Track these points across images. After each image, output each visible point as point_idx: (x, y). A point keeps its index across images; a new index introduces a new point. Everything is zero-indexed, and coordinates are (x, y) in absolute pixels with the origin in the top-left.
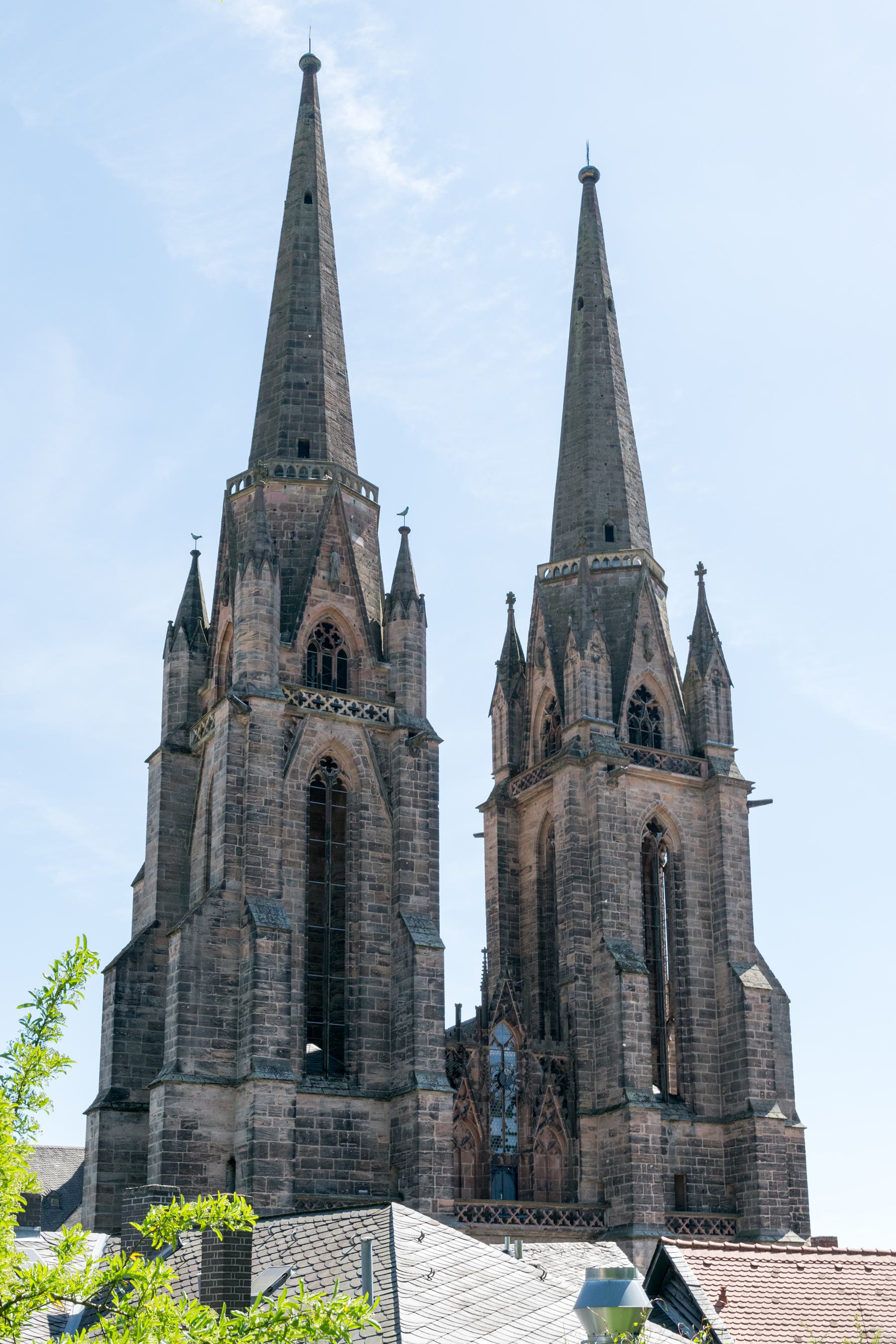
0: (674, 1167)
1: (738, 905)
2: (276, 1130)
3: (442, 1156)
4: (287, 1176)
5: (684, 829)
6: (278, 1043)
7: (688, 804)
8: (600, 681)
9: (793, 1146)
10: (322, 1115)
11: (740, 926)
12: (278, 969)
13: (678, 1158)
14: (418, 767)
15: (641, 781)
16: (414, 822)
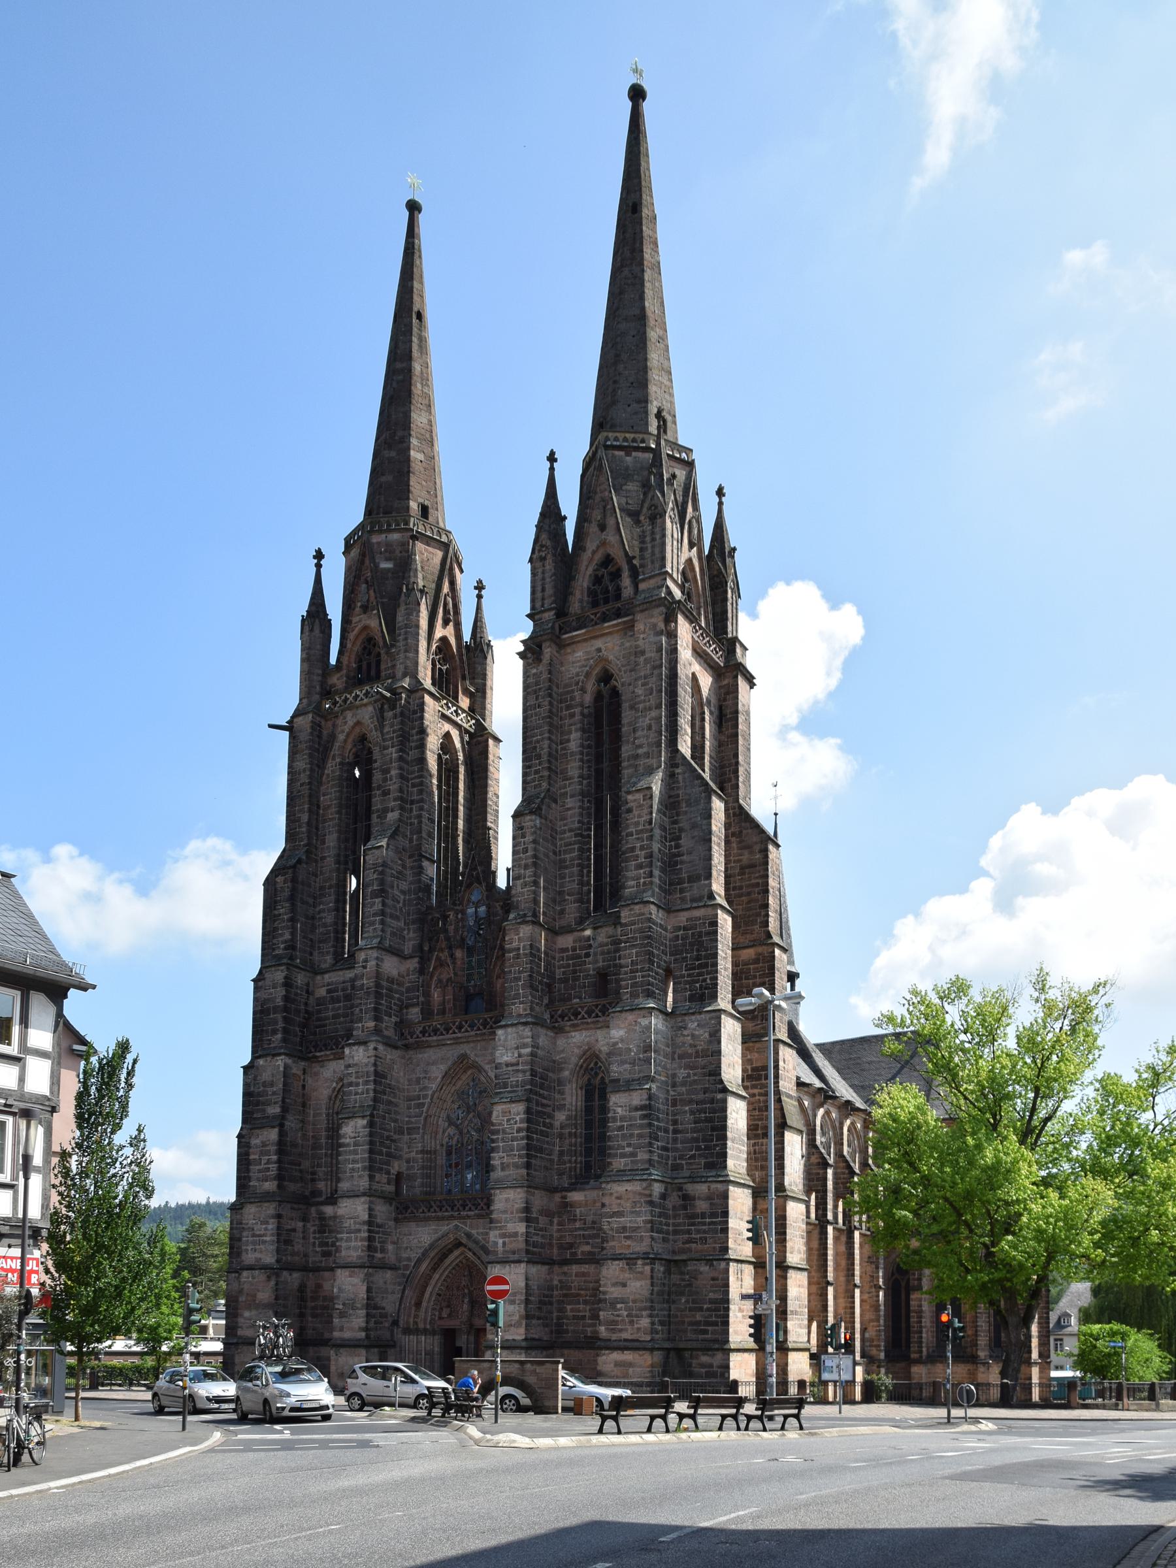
0: (596, 966)
3: (368, 993)
4: (281, 1025)
5: (623, 669)
6: (286, 942)
7: (628, 644)
9: (705, 923)
10: (344, 982)
11: (648, 737)
12: (287, 893)
14: (395, 716)
15: (585, 644)
16: (391, 758)
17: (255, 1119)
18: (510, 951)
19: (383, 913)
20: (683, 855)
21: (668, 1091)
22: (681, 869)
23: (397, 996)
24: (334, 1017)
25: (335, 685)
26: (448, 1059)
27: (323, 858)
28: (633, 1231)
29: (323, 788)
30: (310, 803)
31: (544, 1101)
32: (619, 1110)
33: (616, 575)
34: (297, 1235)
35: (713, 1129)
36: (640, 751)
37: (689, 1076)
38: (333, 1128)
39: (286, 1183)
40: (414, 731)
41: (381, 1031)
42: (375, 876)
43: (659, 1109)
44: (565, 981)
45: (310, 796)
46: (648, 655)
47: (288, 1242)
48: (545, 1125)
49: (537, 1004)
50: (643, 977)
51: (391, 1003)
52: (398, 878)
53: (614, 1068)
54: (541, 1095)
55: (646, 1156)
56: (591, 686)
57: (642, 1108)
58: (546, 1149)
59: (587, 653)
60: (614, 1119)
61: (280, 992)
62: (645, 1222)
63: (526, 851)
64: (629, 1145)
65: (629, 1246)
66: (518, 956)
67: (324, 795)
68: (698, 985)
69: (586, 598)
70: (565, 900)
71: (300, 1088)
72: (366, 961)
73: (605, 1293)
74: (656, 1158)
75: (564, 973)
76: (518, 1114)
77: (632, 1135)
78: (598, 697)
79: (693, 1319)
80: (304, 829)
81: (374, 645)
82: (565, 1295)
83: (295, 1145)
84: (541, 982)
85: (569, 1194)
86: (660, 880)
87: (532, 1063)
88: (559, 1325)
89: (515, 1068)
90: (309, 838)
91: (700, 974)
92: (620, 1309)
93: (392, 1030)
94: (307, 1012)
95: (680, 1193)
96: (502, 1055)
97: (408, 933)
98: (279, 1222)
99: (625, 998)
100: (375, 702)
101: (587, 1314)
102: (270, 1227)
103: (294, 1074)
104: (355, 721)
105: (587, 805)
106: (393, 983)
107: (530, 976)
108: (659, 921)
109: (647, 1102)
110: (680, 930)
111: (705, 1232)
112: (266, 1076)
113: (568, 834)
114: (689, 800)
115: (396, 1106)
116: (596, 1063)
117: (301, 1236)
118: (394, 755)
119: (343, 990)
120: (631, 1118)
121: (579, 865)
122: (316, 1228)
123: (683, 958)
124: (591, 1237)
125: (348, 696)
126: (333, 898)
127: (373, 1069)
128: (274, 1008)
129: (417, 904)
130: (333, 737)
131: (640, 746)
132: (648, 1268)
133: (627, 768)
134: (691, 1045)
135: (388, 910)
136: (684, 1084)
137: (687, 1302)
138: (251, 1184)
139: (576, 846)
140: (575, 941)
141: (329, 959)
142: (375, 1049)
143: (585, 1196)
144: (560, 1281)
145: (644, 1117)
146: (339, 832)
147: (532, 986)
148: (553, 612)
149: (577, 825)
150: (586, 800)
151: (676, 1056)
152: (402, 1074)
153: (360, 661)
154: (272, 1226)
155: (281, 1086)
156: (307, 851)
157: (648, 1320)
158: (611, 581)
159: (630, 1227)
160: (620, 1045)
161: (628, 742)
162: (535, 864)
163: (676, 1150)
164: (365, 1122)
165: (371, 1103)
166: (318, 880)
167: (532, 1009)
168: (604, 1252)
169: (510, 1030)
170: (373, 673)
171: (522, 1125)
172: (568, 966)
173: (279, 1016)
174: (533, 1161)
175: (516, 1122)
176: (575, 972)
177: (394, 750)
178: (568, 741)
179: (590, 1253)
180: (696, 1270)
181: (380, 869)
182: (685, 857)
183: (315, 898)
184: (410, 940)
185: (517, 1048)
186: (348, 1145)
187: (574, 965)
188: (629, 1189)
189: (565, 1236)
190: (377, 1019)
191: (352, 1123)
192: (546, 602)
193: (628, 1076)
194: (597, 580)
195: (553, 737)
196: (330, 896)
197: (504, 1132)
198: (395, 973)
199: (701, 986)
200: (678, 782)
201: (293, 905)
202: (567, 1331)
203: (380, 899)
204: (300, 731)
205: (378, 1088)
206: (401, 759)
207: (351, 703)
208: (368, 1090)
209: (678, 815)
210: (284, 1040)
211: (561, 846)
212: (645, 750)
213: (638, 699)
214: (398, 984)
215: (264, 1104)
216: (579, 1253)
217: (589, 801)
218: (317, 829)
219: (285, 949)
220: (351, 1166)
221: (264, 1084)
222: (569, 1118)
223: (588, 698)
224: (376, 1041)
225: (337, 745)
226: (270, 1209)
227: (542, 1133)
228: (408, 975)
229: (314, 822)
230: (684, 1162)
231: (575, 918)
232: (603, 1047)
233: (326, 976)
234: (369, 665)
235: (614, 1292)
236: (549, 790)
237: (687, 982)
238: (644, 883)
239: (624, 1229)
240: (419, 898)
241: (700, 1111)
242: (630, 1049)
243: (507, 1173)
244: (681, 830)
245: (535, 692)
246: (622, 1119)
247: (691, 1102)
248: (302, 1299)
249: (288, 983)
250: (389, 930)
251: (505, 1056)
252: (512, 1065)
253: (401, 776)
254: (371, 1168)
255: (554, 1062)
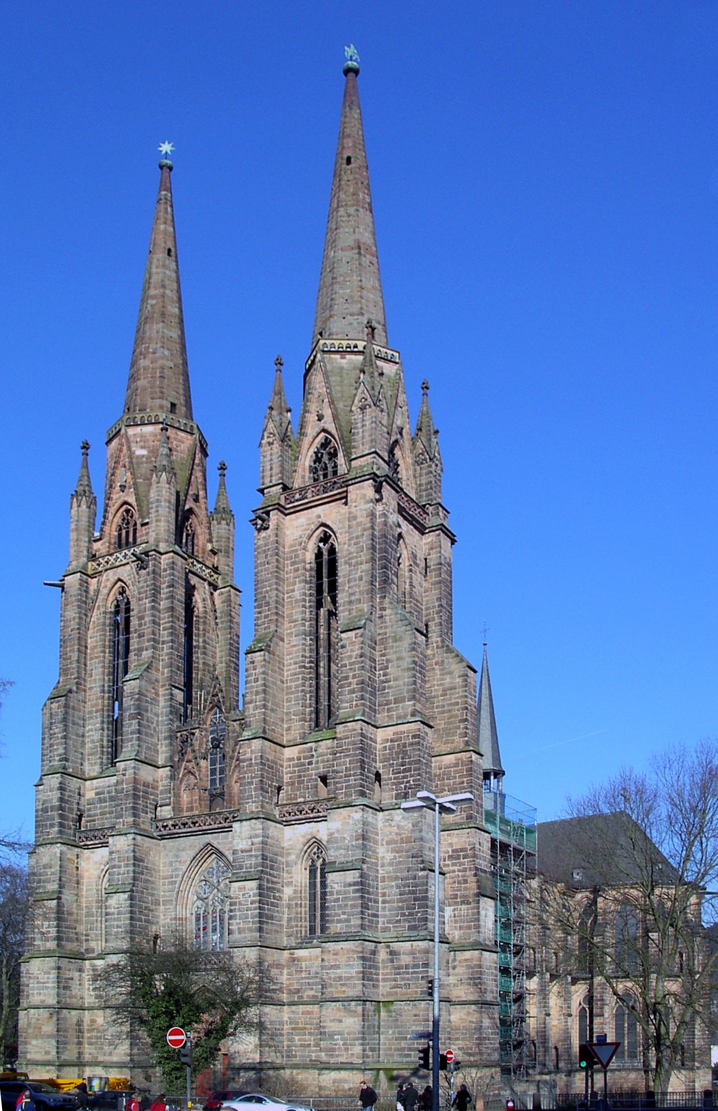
0: (317, 771)
1: (359, 571)
2: (52, 799)
4: (57, 820)
6: (60, 755)
8: (274, 457)
11: (359, 586)
12: (60, 717)
13: (321, 765)
16: (145, 608)
17: (37, 893)
18: (244, 761)
19: (139, 732)
20: (390, 681)
21: (377, 870)
22: (388, 692)
23: (152, 797)
24: (101, 814)
25: (99, 550)
26: (195, 846)
27: (91, 688)
28: (347, 980)
29: (90, 632)
30: (79, 644)
31: (274, 879)
32: (335, 886)
33: (333, 455)
34: (74, 982)
35: (415, 899)
36: (353, 598)
37: (395, 858)
38: (102, 900)
39: (63, 943)
40: (164, 586)
41: (139, 825)
42: (132, 703)
43: (369, 885)
44: (293, 784)
45: (79, 638)
46: (359, 520)
47: (66, 988)
48: (274, 897)
49: (267, 803)
50: (355, 780)
51: (147, 803)
52: (151, 703)
53: (331, 852)
54: (270, 874)
55: (359, 922)
56: (312, 546)
57: (355, 884)
58: (276, 916)
59: (309, 519)
60: (332, 893)
61: (57, 794)
62: (357, 972)
63: (256, 680)
64: (344, 913)
65: (344, 991)
66: (250, 765)
67: (91, 638)
68: (403, 786)
69: (307, 474)
70: (291, 720)
71: (75, 869)
72: (125, 770)
73: (324, 1027)
74: (367, 923)
75: (290, 778)
76: (252, 889)
77: (346, 905)
78: (319, 555)
79: (399, 1046)
80: (74, 666)
81: (132, 517)
82: (293, 1029)
83: (70, 914)
84: (270, 786)
85: (296, 951)
86: (370, 702)
87: (263, 849)
88: (289, 1051)
89: (248, 854)
90: (78, 672)
91: (404, 777)
92: (337, 1039)
93: (149, 825)
94: (79, 810)
95: (388, 950)
96: (238, 844)
97: (162, 747)
98: (58, 973)
99: (340, 797)
100: (133, 562)
101: (312, 1043)
102: (51, 976)
103: (68, 859)
104: (116, 578)
105: (309, 642)
106: (148, 787)
107: (261, 781)
108: (369, 735)
109: (359, 880)
110: (387, 742)
111: (408, 979)
112: (45, 860)
113: (293, 666)
114: (395, 636)
115: (153, 883)
116: (318, 848)
117: (78, 983)
118: (147, 605)
119: (109, 793)
120: (345, 892)
121: (303, 691)
122: (90, 977)
123: (390, 764)
124: (314, 984)
125: (110, 558)
126: (99, 720)
127: (132, 854)
128: (52, 807)
129: (168, 724)
130: (98, 591)
131: (353, 594)
132: (360, 1008)
133: (343, 611)
134: (396, 834)
135: (143, 729)
136: (391, 864)
137: (394, 1033)
138: (35, 943)
139: (300, 676)
140: (300, 752)
141: (97, 768)
142: (134, 839)
143: (310, 953)
144: (289, 1018)
145: (357, 891)
146: (104, 667)
147: (262, 789)
148: (281, 486)
149: (301, 659)
150: (308, 638)
151: (384, 842)
152: (157, 858)
153: (120, 530)
154: (53, 975)
155: (58, 868)
156: (77, 683)
157: (361, 1048)
158: (330, 459)
159: (345, 977)
160: (336, 835)
161: (344, 590)
162: (264, 691)
163: (385, 916)
164: (126, 896)
165: (131, 881)
166: (86, 706)
167: (262, 807)
168: (324, 996)
169: (244, 823)
170: (131, 539)
171: (255, 898)
172: (294, 772)
173: (55, 813)
174: (265, 926)
175: (250, 896)
176: (300, 777)
177: (147, 600)
178: (293, 591)
179: (314, 996)
180: (401, 1009)
181: (137, 696)
182: (392, 683)
183: (84, 720)
184: (163, 753)
185: (251, 838)
186: (113, 914)
187: (299, 771)
188: (344, 947)
189: (293, 984)
190: (135, 815)
191: (116, 896)
192: (274, 478)
193: (343, 860)
194: (318, 459)
195: (280, 588)
196: (96, 718)
197: (240, 904)
198: (150, 779)
199: (405, 787)
200: (385, 622)
201: (65, 725)
202: (295, 1056)
203: (137, 720)
204: (70, 587)
205: (137, 869)
206: (153, 608)
207: (113, 563)
208: (128, 871)
209: (385, 649)
210: (60, 832)
211: (288, 676)
212: (357, 597)
213: (351, 556)
214: (152, 788)
215: (44, 882)
216: (305, 997)
217: (311, 639)
218: (85, 665)
219: (60, 761)
220: (115, 930)
221: (45, 867)
222: (295, 892)
223: (310, 556)
224: (134, 833)
225: (100, 597)
226: (51, 962)
227: (273, 904)
228: (162, 780)
229: (83, 661)
230: (391, 926)
231: (300, 734)
232: (323, 837)
233: (95, 781)
234: (127, 533)
235: (331, 1027)
236: (276, 631)
237: (393, 784)
238: (356, 704)
239: (340, 978)
240: (171, 720)
241: (404, 886)
242: (345, 838)
243: (243, 935)
244: (388, 661)
245: (265, 551)
246: (338, 893)
247: (397, 878)
248: (80, 1031)
249: (62, 788)
250: (144, 745)
251: (242, 845)
252: (246, 851)
253: (154, 622)
254: (132, 932)
255: (283, 848)
